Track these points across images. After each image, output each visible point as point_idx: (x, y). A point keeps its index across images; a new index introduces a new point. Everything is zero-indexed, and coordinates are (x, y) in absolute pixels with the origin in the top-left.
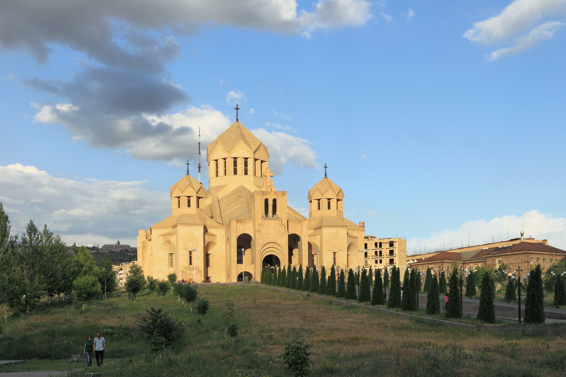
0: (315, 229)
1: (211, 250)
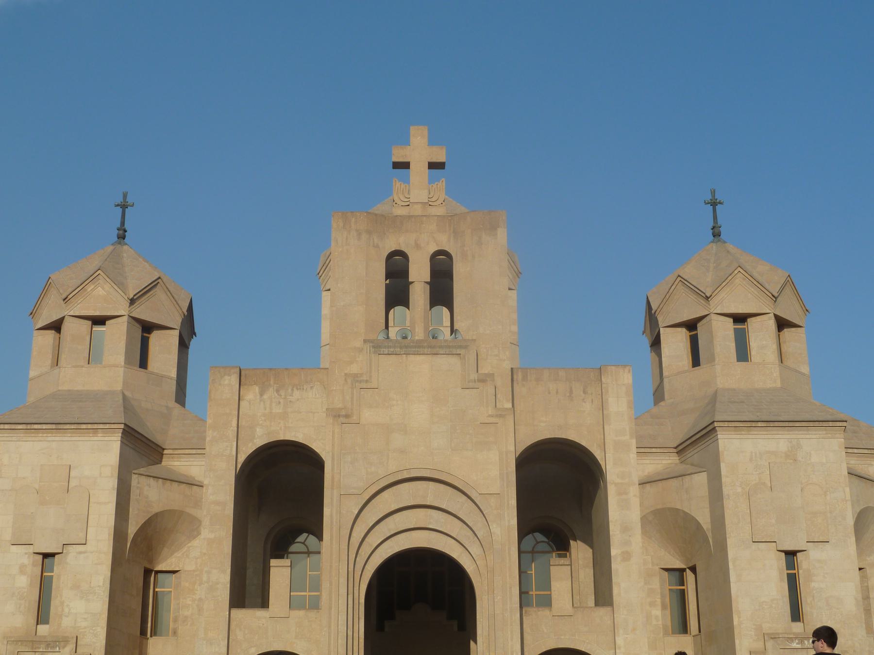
0: (681, 449)
1: (178, 554)
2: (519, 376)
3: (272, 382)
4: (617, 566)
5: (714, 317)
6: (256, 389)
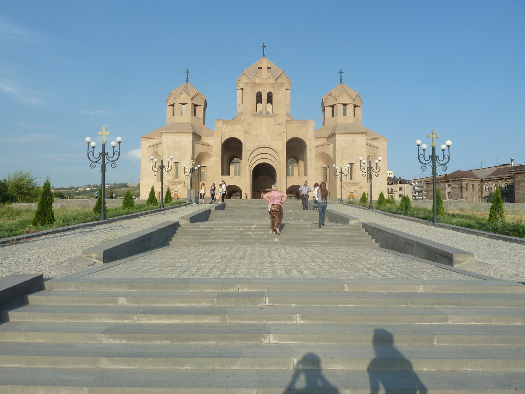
0: (328, 138)
2: (288, 122)
3: (229, 123)
4: (309, 167)
5: (338, 104)
6: (226, 125)
